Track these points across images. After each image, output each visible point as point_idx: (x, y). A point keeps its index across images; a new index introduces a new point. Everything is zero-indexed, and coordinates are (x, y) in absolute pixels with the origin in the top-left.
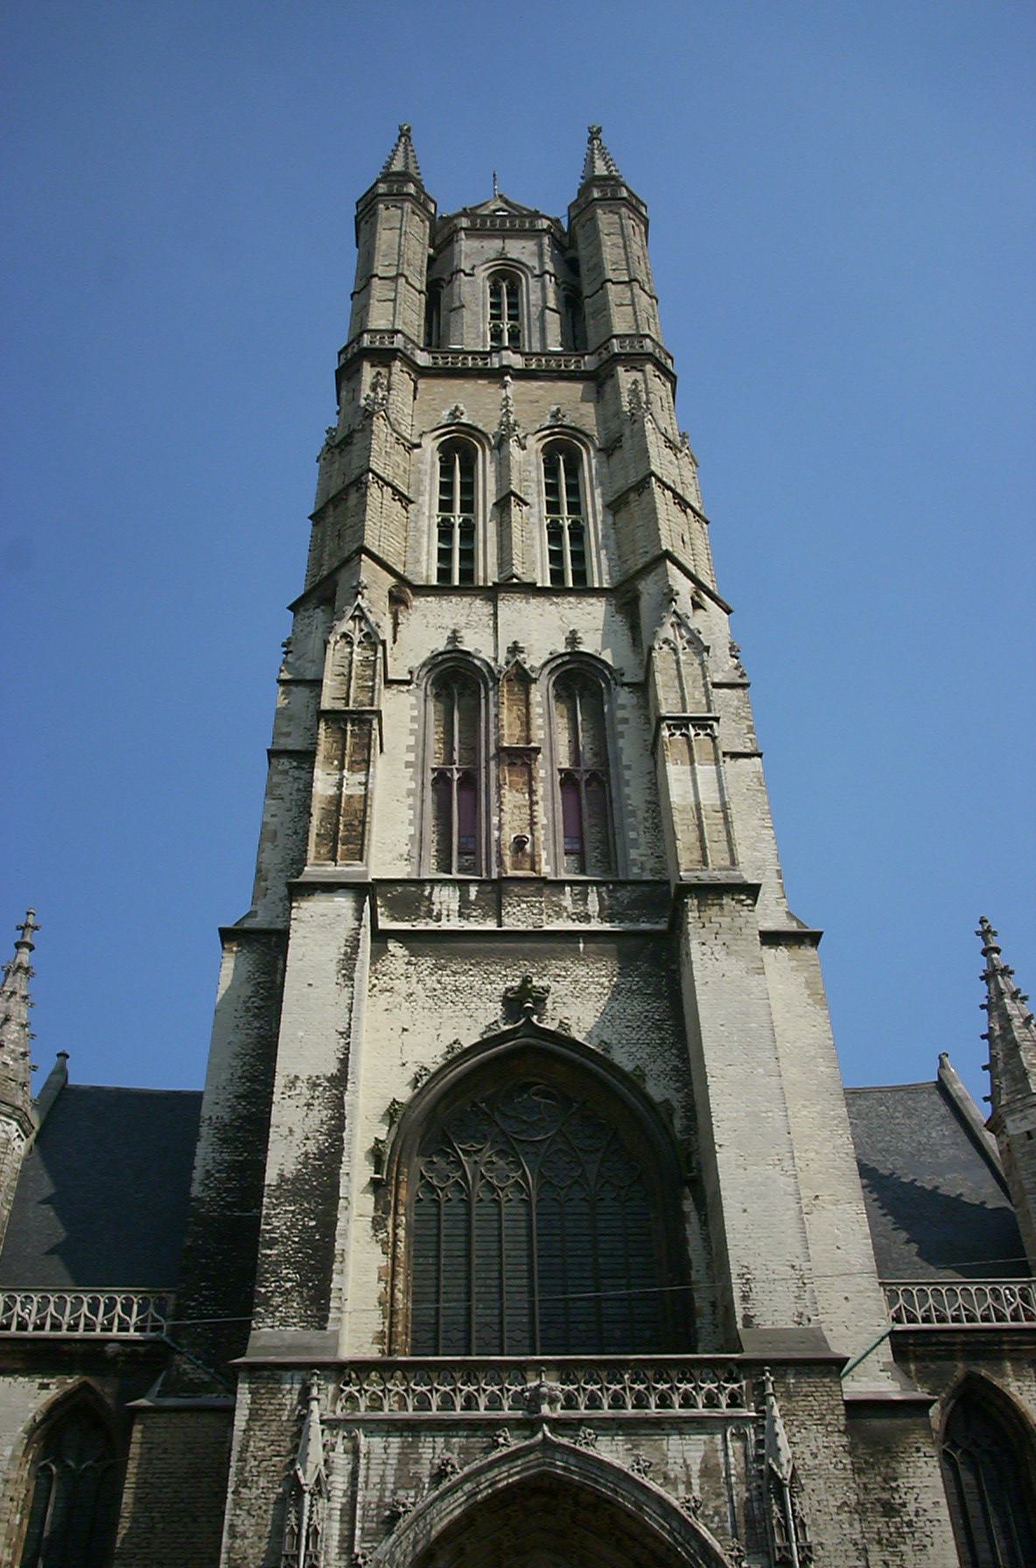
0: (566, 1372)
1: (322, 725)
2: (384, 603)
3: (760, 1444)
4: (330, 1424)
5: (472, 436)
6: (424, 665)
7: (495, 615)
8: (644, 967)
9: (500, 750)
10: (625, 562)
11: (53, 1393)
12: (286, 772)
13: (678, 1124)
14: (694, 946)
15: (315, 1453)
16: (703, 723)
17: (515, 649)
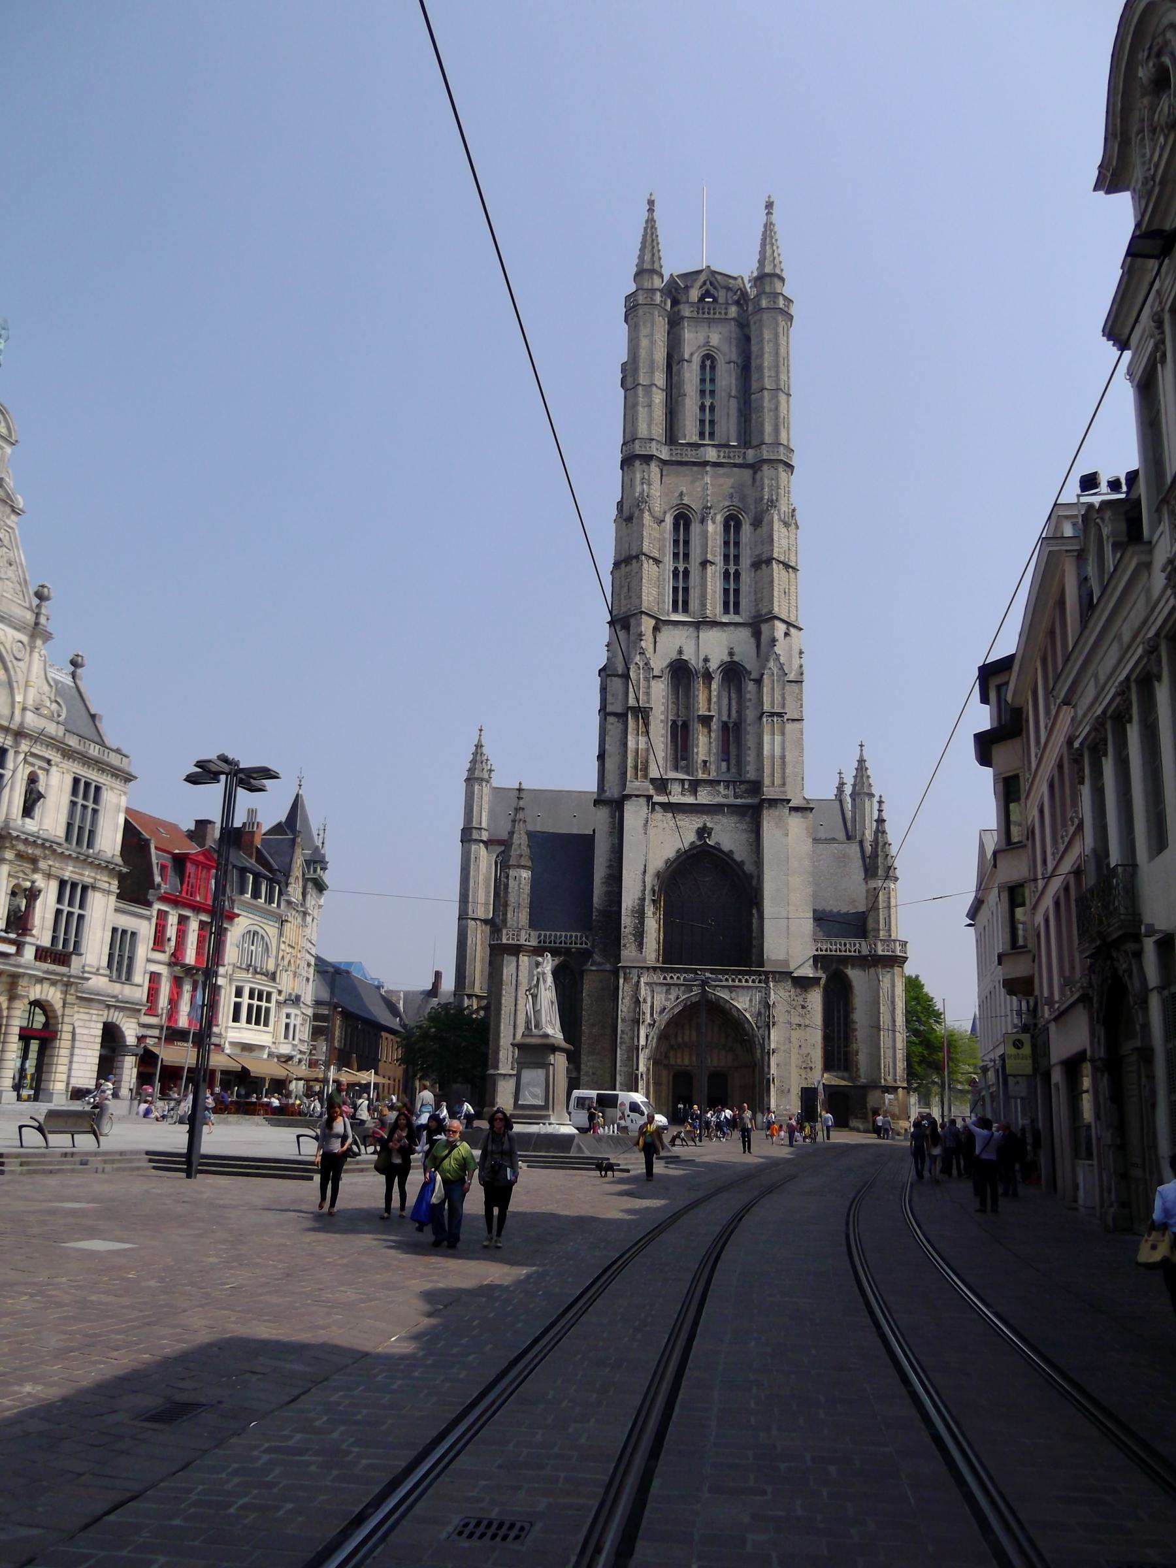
0: (712, 972)
1: (629, 712)
2: (650, 631)
3: (766, 994)
4: (646, 984)
5: (688, 511)
6: (667, 667)
7: (698, 637)
8: (748, 819)
10: (758, 604)
12: (612, 724)
13: (754, 882)
14: (765, 823)
15: (643, 992)
16: (780, 715)
17: (706, 660)
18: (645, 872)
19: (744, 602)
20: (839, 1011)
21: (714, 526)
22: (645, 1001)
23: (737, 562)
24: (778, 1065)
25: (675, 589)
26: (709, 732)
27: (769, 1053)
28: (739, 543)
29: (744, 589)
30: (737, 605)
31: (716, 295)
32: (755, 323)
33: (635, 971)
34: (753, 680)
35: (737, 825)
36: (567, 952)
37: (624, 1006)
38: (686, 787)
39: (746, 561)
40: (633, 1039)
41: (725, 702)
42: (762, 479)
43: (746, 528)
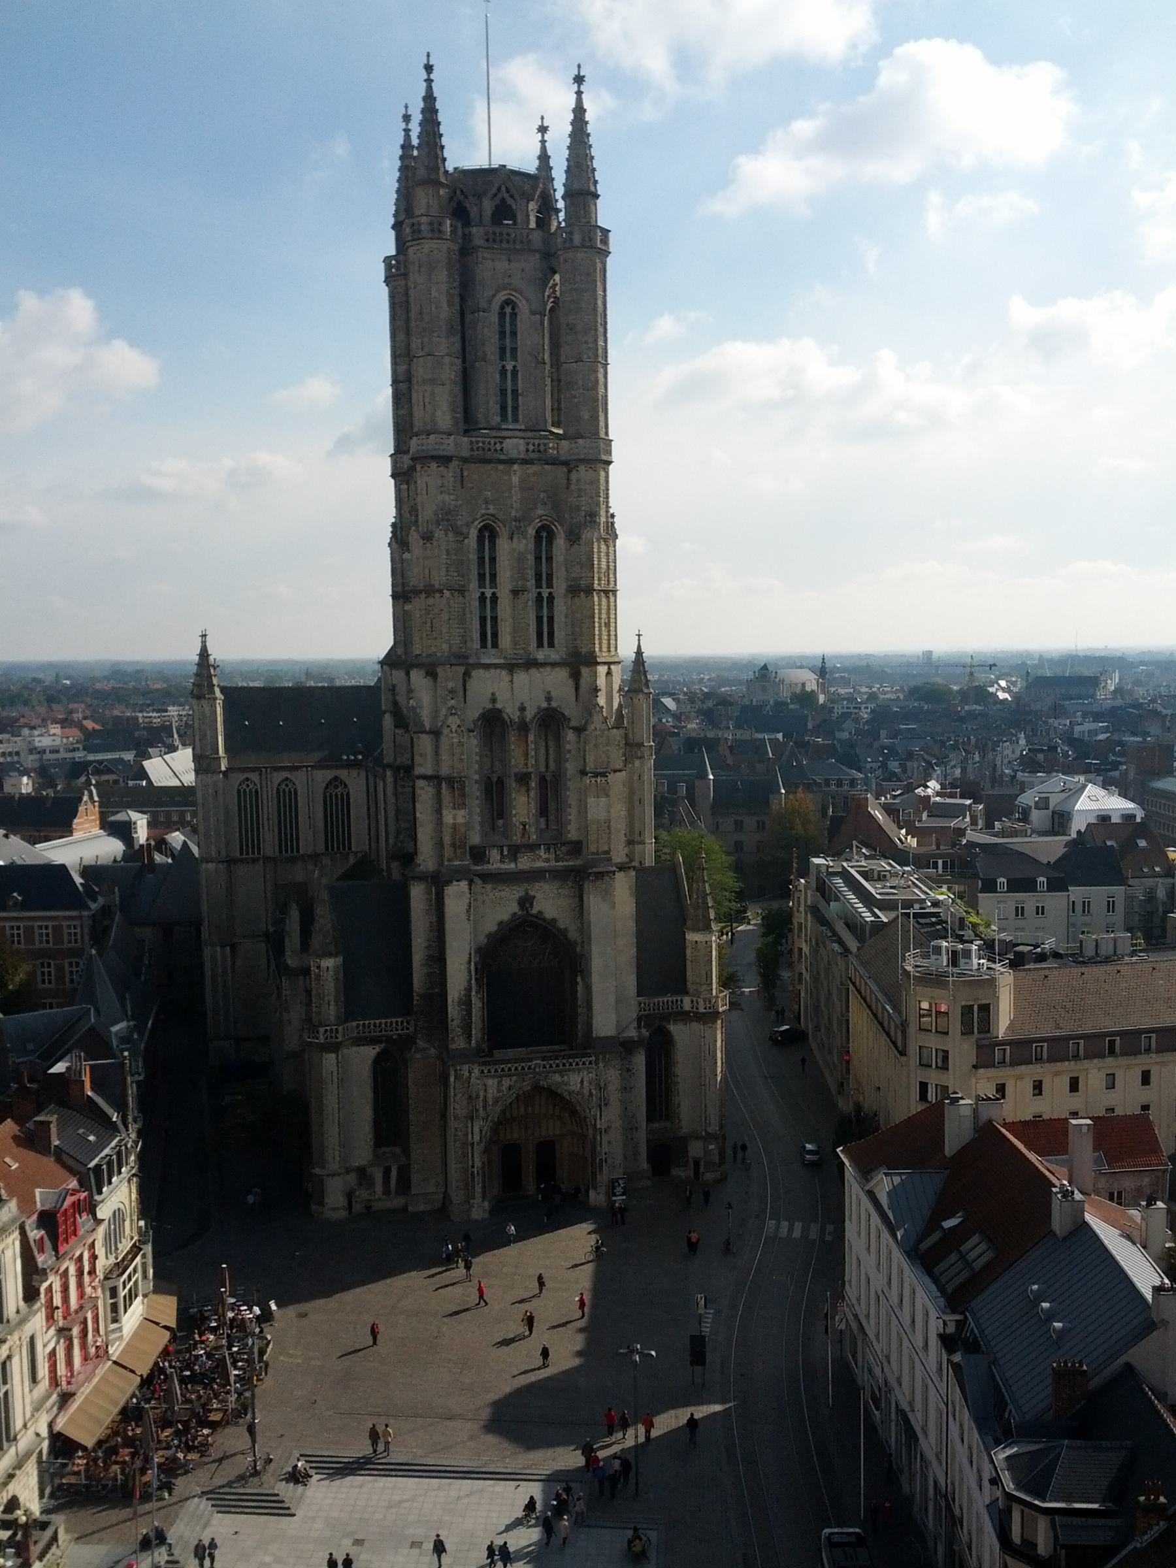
6: (479, 719)
7: (511, 681)
8: (570, 884)
9: (516, 775)
10: (576, 640)
11: (378, 1049)
13: (578, 949)
17: (522, 709)
18: (470, 962)
19: (559, 635)
20: (660, 1063)
21: (524, 541)
22: (478, 1096)
23: (550, 585)
24: (609, 1142)
25: (483, 619)
26: (528, 791)
27: (601, 1133)
28: (552, 558)
29: (559, 620)
30: (551, 635)
31: (514, 207)
32: (566, 261)
33: (466, 1067)
34: (572, 728)
35: (560, 891)
36: (389, 1039)
37: (458, 1106)
38: (506, 853)
39: (560, 586)
40: (467, 1135)
41: (543, 750)
42: (578, 481)
43: (560, 543)
